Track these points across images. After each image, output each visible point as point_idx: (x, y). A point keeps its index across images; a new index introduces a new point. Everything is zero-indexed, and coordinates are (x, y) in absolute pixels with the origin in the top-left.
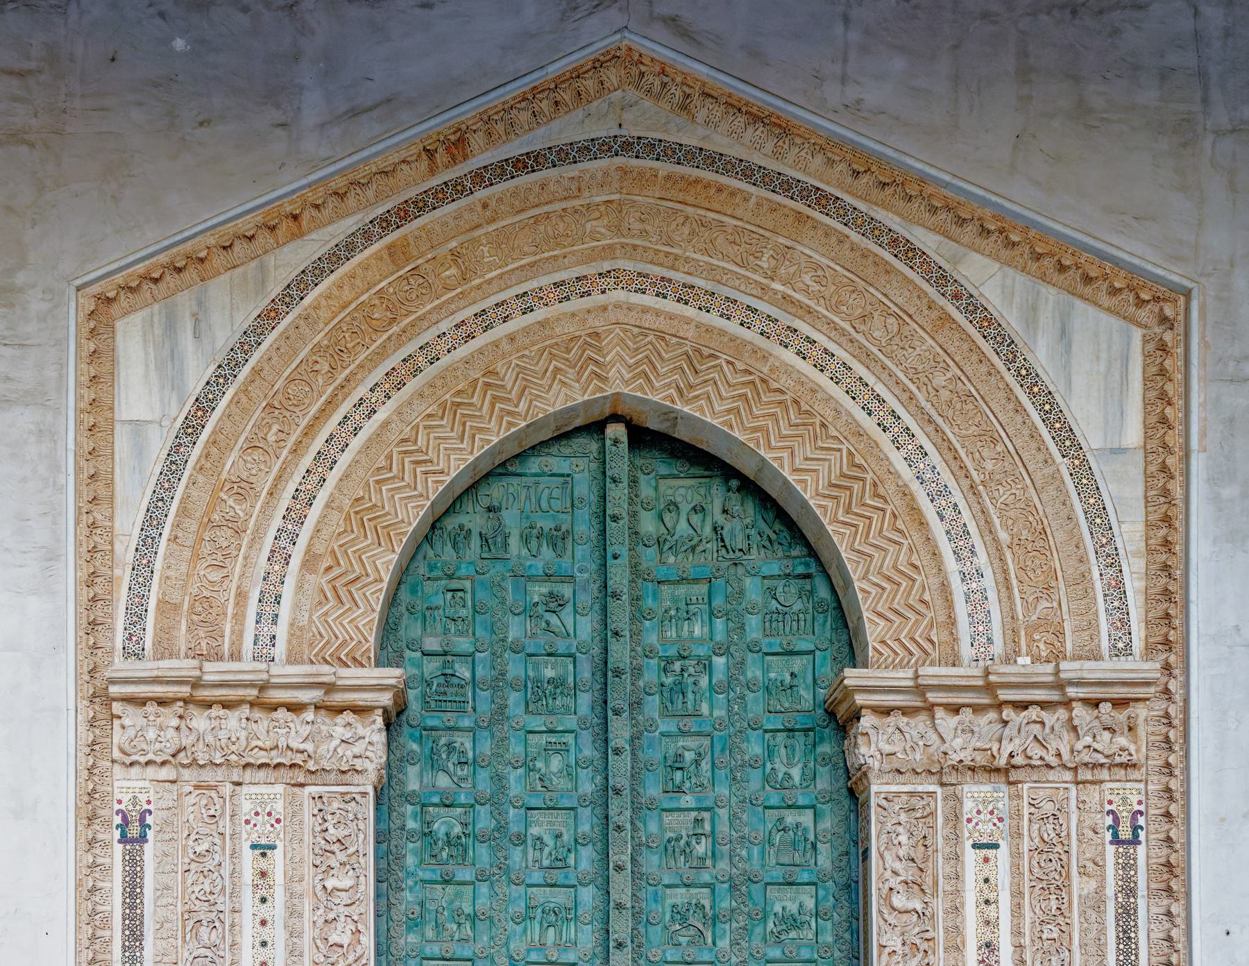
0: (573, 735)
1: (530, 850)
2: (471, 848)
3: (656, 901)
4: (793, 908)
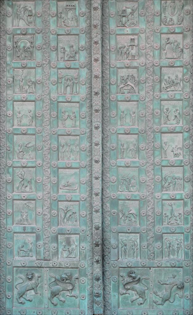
1: (59, 53)
2: (34, 53)
3: (114, 74)
4: (173, 78)
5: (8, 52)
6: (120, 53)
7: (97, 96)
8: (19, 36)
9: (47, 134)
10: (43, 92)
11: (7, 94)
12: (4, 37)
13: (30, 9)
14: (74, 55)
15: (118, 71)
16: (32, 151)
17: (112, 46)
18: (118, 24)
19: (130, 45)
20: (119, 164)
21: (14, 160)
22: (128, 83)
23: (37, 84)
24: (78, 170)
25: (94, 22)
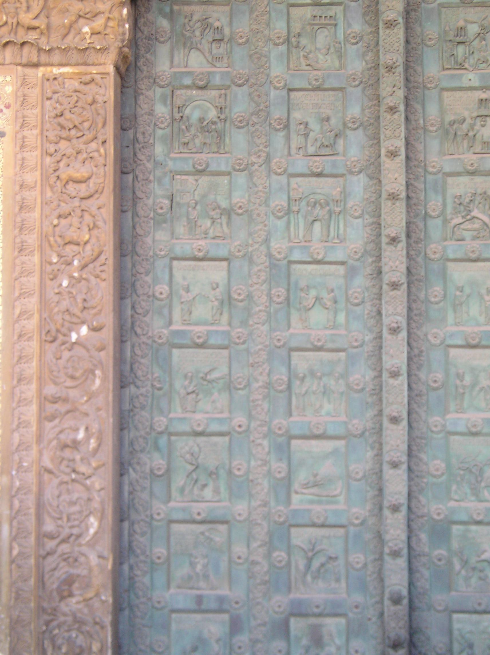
0: (341, 8)
5: (160, 132)
6: (451, 136)
7: (395, 247)
8: (189, 92)
9: (260, 347)
10: (250, 234)
11: (154, 241)
12: (150, 93)
13: (217, 24)
14: (332, 142)
15: (445, 183)
16: (220, 391)
17: (431, 118)
18: (445, 63)
19: (478, 116)
20: (450, 428)
21: (172, 415)
22: (473, 214)
23: (234, 216)
24: (343, 442)
25: (385, 58)
